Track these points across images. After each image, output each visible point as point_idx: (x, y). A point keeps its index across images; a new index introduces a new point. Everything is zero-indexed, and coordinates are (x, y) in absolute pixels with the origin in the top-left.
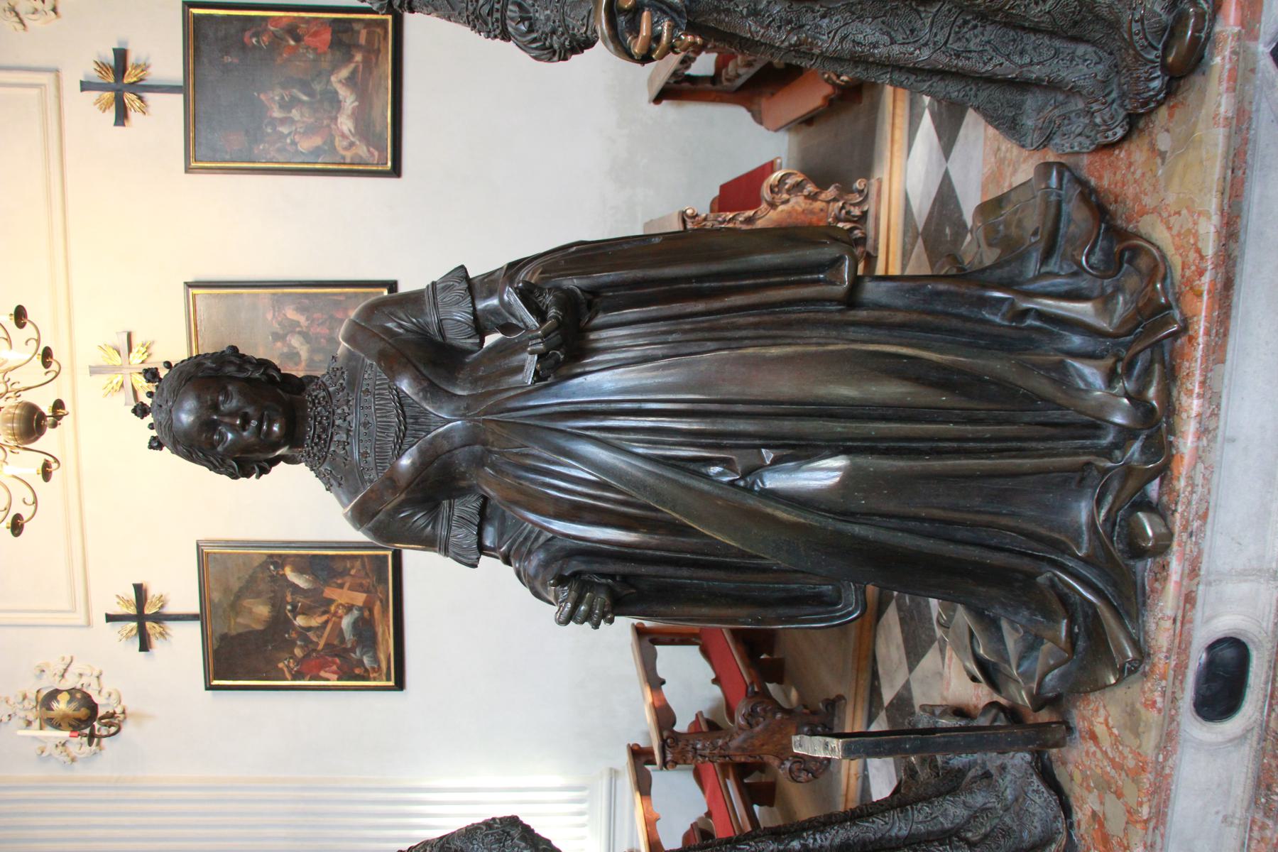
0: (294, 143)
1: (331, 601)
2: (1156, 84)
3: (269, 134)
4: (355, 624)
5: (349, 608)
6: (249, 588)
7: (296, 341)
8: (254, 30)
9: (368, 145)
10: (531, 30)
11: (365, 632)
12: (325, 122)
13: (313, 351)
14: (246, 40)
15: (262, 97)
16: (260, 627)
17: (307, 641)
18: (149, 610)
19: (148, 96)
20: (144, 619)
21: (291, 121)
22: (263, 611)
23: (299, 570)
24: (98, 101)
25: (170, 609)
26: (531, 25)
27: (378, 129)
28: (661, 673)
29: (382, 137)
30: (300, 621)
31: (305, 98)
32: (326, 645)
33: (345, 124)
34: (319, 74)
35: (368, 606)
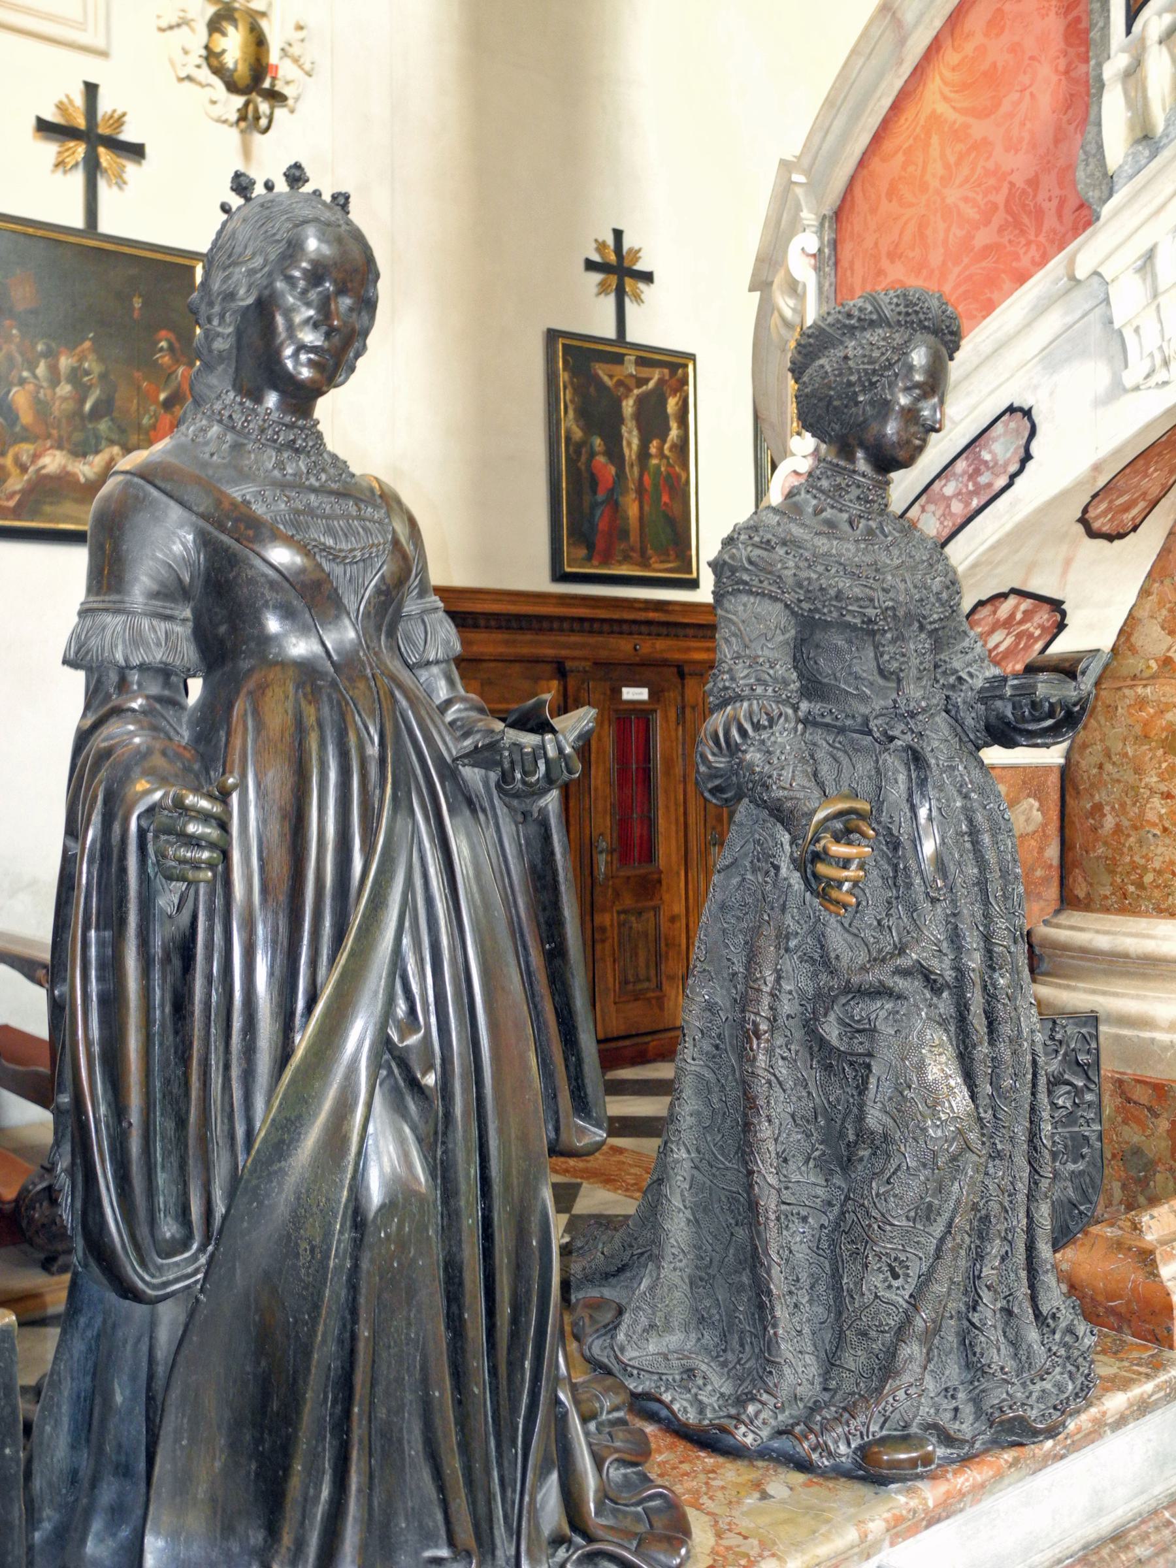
0: (22, 382)
2: (843, 1449)
3: (34, 346)
8: (177, 345)
9: (23, 492)
10: (757, 727)
12: (54, 432)
14: (163, 333)
15: (87, 344)
19: (78, 179)
21: (55, 381)
24: (71, 101)
26: (765, 728)
27: (48, 509)
29: (34, 514)
31: (88, 406)
33: (53, 462)
34: (122, 431)
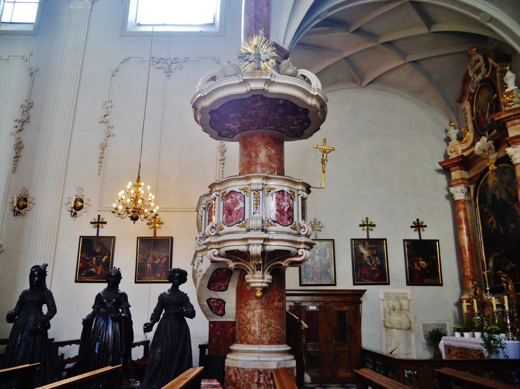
1: (99, 266)
4: (93, 272)
5: (96, 270)
6: (103, 248)
7: (158, 260)
11: (91, 274)
13: (156, 264)
16: (94, 249)
17: (90, 260)
18: (100, 225)
20: (98, 223)
22: (98, 250)
23: (106, 259)
25: (100, 229)
28: (73, 345)
30: (94, 259)
32: (88, 265)
35: (96, 275)
